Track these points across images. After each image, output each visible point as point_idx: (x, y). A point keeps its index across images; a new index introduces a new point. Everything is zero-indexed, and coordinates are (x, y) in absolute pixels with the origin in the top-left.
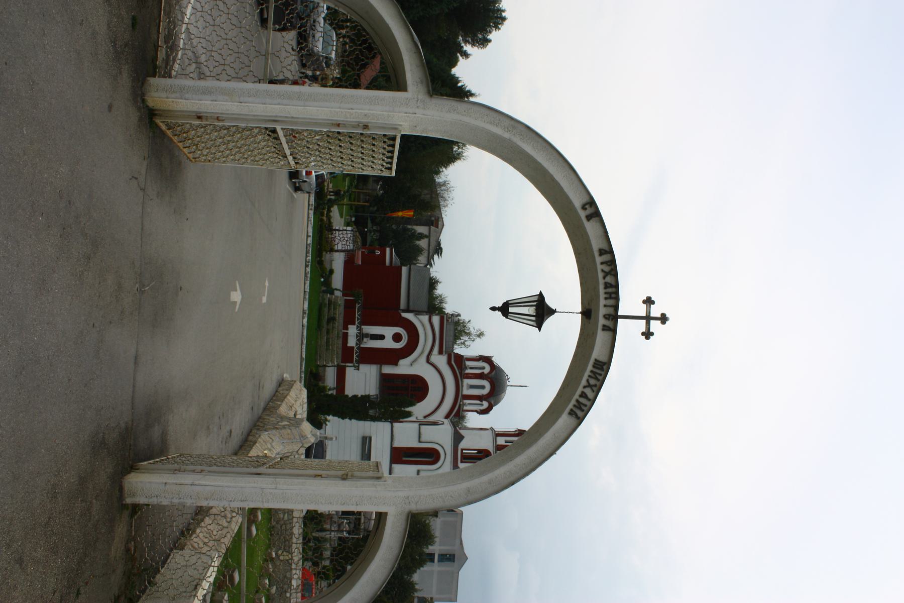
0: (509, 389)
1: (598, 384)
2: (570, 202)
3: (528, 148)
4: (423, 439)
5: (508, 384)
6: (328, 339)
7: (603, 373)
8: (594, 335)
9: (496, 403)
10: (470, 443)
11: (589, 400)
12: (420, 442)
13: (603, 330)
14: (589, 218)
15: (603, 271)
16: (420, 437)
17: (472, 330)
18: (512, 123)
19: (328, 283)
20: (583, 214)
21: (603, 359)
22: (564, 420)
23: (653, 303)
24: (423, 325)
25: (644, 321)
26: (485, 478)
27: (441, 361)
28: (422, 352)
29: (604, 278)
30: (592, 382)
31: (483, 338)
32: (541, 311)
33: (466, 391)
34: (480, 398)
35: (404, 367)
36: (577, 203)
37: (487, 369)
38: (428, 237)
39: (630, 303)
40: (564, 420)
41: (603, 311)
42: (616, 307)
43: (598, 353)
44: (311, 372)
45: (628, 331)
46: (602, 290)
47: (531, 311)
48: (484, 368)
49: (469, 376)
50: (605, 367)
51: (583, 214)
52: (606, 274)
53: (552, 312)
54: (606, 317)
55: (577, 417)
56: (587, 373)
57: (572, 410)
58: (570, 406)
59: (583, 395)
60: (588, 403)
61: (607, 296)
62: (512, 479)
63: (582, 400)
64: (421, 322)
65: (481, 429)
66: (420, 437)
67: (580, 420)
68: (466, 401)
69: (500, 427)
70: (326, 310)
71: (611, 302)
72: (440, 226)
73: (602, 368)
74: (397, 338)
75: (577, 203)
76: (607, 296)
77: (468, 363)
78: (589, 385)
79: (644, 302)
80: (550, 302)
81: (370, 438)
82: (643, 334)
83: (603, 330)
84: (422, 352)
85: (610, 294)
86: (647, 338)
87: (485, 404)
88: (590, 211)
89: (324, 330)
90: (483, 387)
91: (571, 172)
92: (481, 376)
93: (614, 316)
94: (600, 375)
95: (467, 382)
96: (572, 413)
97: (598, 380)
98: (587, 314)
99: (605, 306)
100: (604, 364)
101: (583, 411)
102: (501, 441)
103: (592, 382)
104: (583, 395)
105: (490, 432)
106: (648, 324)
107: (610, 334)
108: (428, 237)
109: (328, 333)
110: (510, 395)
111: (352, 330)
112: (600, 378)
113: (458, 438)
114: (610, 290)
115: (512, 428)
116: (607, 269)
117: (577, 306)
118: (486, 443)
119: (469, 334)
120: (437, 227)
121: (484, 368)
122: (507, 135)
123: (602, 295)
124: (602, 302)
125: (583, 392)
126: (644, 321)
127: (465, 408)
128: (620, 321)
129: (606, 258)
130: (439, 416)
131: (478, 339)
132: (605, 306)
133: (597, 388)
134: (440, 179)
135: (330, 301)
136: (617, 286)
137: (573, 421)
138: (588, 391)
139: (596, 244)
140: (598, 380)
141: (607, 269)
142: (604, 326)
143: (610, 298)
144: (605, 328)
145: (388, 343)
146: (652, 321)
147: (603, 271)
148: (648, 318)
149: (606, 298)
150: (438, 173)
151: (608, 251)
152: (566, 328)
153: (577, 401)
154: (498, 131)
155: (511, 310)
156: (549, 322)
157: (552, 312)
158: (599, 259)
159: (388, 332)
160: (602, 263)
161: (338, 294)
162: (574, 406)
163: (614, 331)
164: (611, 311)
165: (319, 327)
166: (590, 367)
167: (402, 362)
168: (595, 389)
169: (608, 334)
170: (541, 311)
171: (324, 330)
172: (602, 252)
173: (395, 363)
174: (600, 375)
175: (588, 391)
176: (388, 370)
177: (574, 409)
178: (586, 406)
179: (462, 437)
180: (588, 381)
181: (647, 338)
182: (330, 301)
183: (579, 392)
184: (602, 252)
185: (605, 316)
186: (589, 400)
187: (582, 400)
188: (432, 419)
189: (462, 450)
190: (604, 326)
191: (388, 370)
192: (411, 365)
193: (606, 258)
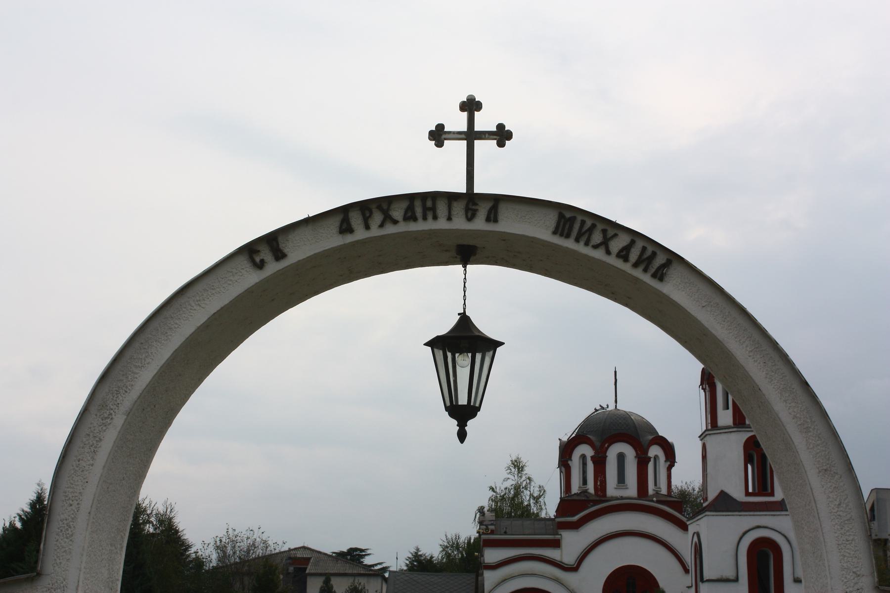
0: (624, 406)
1: (600, 227)
2: (249, 292)
3: (145, 376)
4: (731, 574)
5: (612, 407)
7: (580, 218)
8: (506, 238)
9: (651, 429)
10: (733, 479)
11: (633, 242)
12: (736, 580)
13: (496, 221)
14: (279, 255)
15: (381, 226)
17: (509, 484)
18: (93, 409)
20: (273, 267)
21: (552, 219)
22: (673, 289)
23: (440, 127)
24: (504, 580)
25: (477, 143)
26: (798, 439)
27: (573, 543)
28: (557, 580)
29: (395, 222)
30: (597, 238)
31: (524, 460)
32: (464, 342)
33: (631, 490)
34: (643, 462)
36: (251, 278)
37: (586, 450)
38: (327, 578)
39: (442, 172)
40: (673, 289)
41: (460, 223)
42: (451, 197)
43: (541, 230)
45: (497, 174)
46: (420, 226)
47: (463, 362)
48: (583, 457)
49: (601, 485)
50: (568, 215)
51: (273, 267)
52: (388, 219)
53: (464, 320)
54: (470, 216)
55: (667, 264)
56: (581, 248)
57: (654, 276)
58: (647, 278)
59: (624, 254)
60: (639, 244)
61: (430, 216)
62: (796, 386)
63: (634, 255)
65: (704, 457)
67: (673, 258)
68: (651, 491)
69: (698, 421)
72: (306, 555)
73: (568, 219)
75: (251, 278)
76: (430, 216)
77: (575, 489)
78: (605, 245)
79: (440, 144)
80: (445, 325)
82: (501, 144)
83: (496, 221)
84: (557, 580)
85: (425, 210)
86: (509, 135)
87: (655, 451)
88: (265, 254)
90: (621, 457)
91: (190, 293)
92: (600, 463)
93: (470, 201)
94: (583, 223)
95: (612, 490)
96: (660, 275)
97: (594, 226)
98: (465, 253)
99: (449, 219)
100: (561, 216)
101: (654, 254)
102: (725, 417)
103: (597, 238)
104: (624, 254)
105: (709, 440)
106: (484, 135)
108: (327, 578)
110: (634, 403)
112: (589, 223)
113: (724, 503)
114: (419, 211)
115: (699, 397)
116: (377, 218)
118: (731, 447)
119: (518, 489)
120: (308, 559)
121: (583, 457)
122: (119, 421)
124: (442, 224)
125: (619, 255)
126: (477, 143)
127: (664, 491)
128: (477, 190)
129: (356, 220)
130: (682, 542)
131: (527, 471)
132: (449, 219)
133: (610, 228)
134: (212, 557)
136: (411, 198)
137: (675, 272)
138: (616, 245)
139: (331, 239)
140: (594, 226)
141: (377, 218)
142: (488, 220)
143: (433, 209)
144: (492, 217)
147: (381, 226)
148: (471, 136)
149: (435, 218)
150: (199, 562)
151: (343, 217)
152: (496, 294)
153: (636, 265)
154: (110, 437)
155: (463, 400)
156: (486, 326)
157: (464, 320)
158: (360, 234)
160: (367, 227)
162: (645, 270)
163: (497, 200)
164: (459, 208)
166: (569, 244)
168: (611, 232)
169: (504, 210)
170: (464, 342)
174: (583, 223)
175: (616, 245)
177: (653, 270)
178: (644, 249)
179: (723, 495)
180: (596, 247)
181: (509, 135)
183: (619, 264)
184: (346, 228)
185: (470, 218)
186: (633, 242)
187: (634, 255)
188: (688, 557)
189: (747, 494)
190: (488, 220)
193: (356, 220)
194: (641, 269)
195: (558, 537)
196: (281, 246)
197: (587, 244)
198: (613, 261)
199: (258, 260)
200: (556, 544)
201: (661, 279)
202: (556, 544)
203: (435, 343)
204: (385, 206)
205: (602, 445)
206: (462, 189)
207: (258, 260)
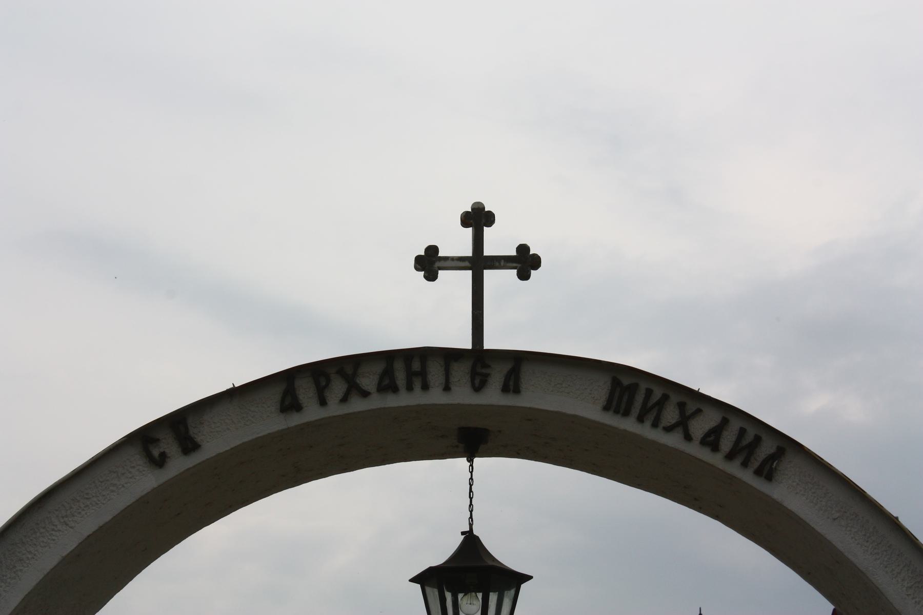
1: (675, 398)
2: (143, 501)
7: (643, 386)
8: (533, 416)
11: (725, 422)
13: (517, 391)
14: (189, 446)
20: (179, 464)
21: (601, 387)
25: (488, 274)
29: (365, 394)
30: (671, 415)
36: (147, 481)
39: (435, 318)
40: (788, 493)
41: (462, 395)
43: (586, 405)
45: (519, 320)
50: (626, 381)
51: (179, 464)
52: (354, 389)
53: (471, 542)
55: (779, 454)
56: (646, 431)
57: (758, 472)
58: (747, 476)
59: (711, 440)
60: (735, 425)
61: (417, 385)
63: (727, 441)
67: (787, 447)
71: (435, 373)
73: (627, 387)
75: (147, 481)
76: (417, 385)
78: (682, 425)
79: (431, 276)
80: (441, 550)
82: (524, 275)
83: (517, 391)
85: (411, 376)
86: (535, 262)
88: (168, 444)
93: (478, 361)
94: (649, 392)
96: (767, 472)
97: (665, 397)
98: (472, 442)
99: (447, 388)
100: (616, 383)
103: (671, 415)
104: (711, 440)
106: (498, 262)
107: (527, 371)
112: (658, 393)
114: (400, 377)
116: (338, 388)
117: (456, 467)
123: (417, 398)
124: (436, 397)
125: (704, 442)
126: (488, 274)
128: (490, 343)
129: (306, 391)
132: (447, 388)
137: (789, 466)
138: (700, 426)
139: (269, 422)
140: (665, 397)
141: (338, 388)
142: (505, 389)
143: (423, 374)
144: (512, 385)
146: (488, 251)
147: (344, 400)
148: (478, 263)
151: (286, 386)
153: (730, 457)
156: (504, 550)
157: (471, 542)
158: (312, 413)
160: (323, 402)
162: (745, 464)
163: (518, 362)
164: (461, 372)
166: (629, 425)
168: (691, 407)
170: (470, 575)
172: (290, 404)
174: (649, 392)
175: (700, 426)
177: (756, 465)
178: (742, 431)
180: (668, 429)
181: (535, 262)
183: (705, 454)
184: (290, 404)
186: (725, 422)
187: (727, 441)
190: (505, 389)
193: (306, 391)
194: (737, 462)
196: (192, 432)
197: (655, 425)
198: (695, 450)
199: (156, 453)
201: (769, 478)
203: (425, 579)
204: (349, 370)
206: (467, 344)
207: (156, 453)
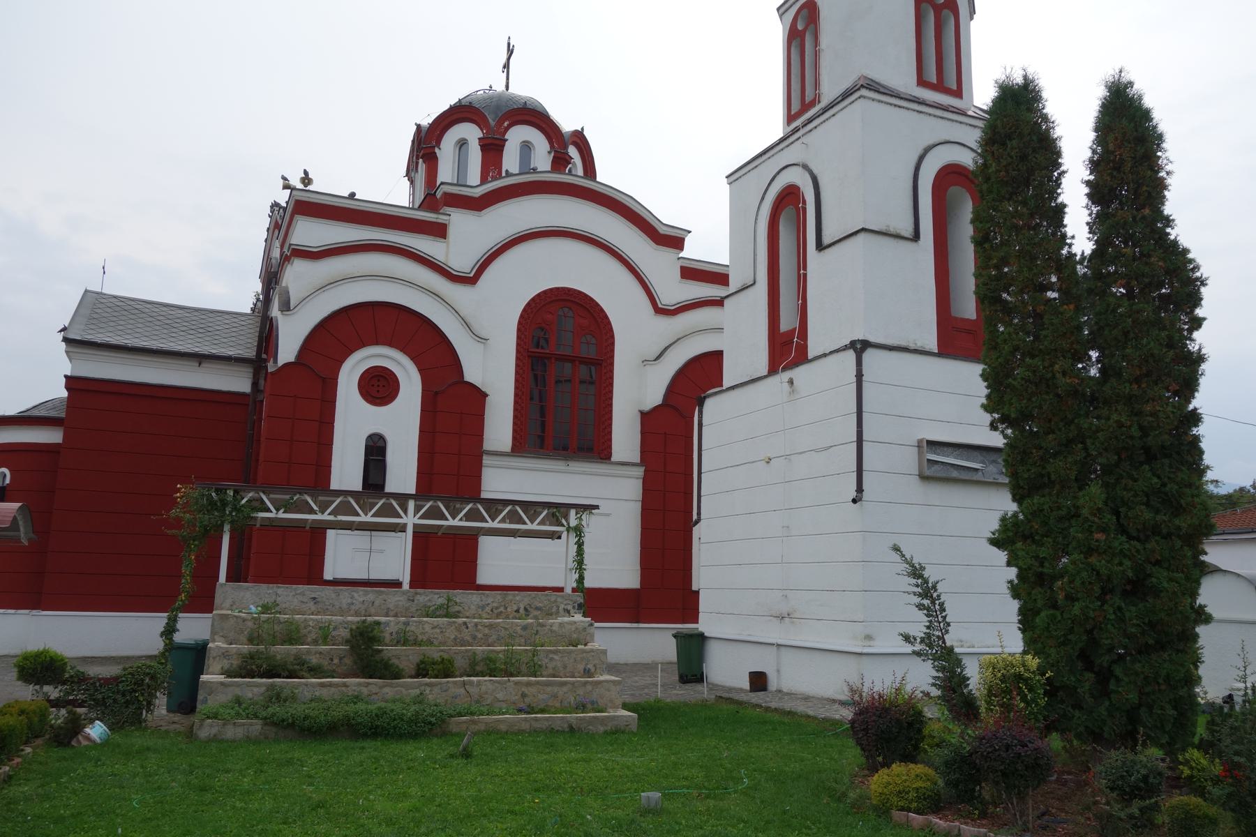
6: (489, 667)
16: (898, 236)
19: (121, 694)
27: (468, 236)
35: (492, 367)
37: (470, 132)
44: (933, 804)
64: (316, 296)
66: (898, 236)
70: (308, 686)
74: (379, 387)
81: (932, 444)
87: (573, 151)
89: (437, 692)
90: (526, 147)
109: (445, 670)
111: (345, 555)
121: (462, 143)
135: (248, 668)
145: (401, 423)
159: (353, 420)
161: (192, 628)
165: (422, 727)
167: (472, 374)
171: (437, 692)
173: (477, 397)
176: (499, 427)
182: (248, 668)
189: (922, 82)
191: (499, 427)
192: (482, 340)
195: (442, 219)
200: (440, 231)
202: (440, 231)
205: (500, 122)
